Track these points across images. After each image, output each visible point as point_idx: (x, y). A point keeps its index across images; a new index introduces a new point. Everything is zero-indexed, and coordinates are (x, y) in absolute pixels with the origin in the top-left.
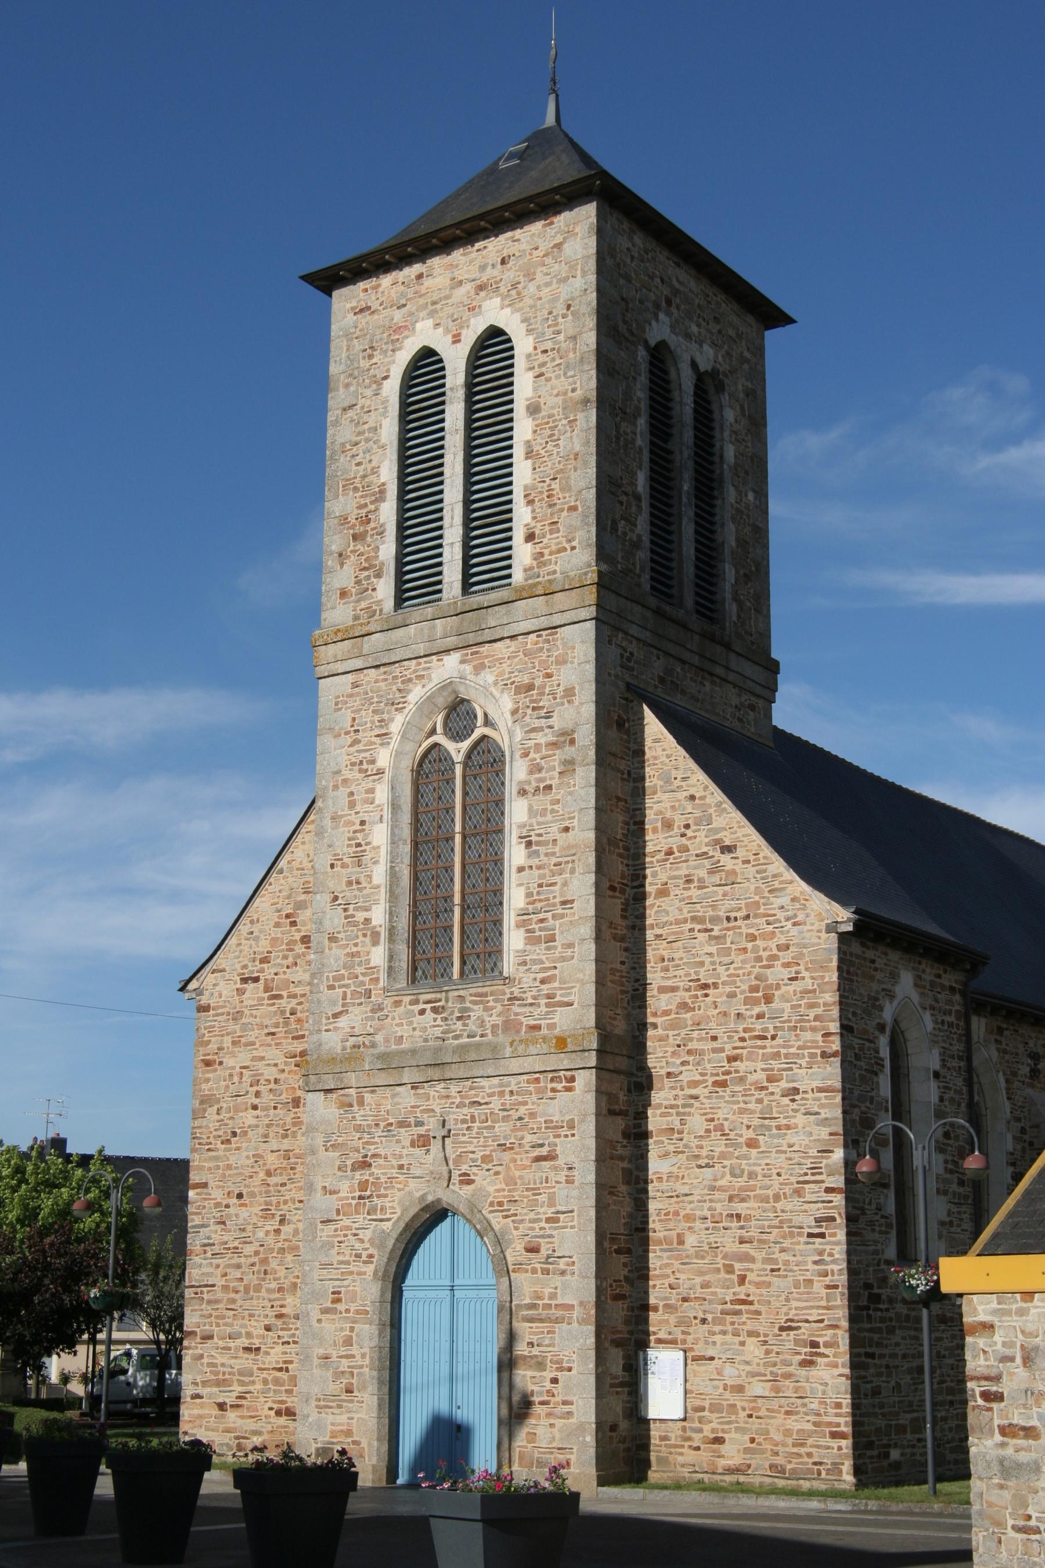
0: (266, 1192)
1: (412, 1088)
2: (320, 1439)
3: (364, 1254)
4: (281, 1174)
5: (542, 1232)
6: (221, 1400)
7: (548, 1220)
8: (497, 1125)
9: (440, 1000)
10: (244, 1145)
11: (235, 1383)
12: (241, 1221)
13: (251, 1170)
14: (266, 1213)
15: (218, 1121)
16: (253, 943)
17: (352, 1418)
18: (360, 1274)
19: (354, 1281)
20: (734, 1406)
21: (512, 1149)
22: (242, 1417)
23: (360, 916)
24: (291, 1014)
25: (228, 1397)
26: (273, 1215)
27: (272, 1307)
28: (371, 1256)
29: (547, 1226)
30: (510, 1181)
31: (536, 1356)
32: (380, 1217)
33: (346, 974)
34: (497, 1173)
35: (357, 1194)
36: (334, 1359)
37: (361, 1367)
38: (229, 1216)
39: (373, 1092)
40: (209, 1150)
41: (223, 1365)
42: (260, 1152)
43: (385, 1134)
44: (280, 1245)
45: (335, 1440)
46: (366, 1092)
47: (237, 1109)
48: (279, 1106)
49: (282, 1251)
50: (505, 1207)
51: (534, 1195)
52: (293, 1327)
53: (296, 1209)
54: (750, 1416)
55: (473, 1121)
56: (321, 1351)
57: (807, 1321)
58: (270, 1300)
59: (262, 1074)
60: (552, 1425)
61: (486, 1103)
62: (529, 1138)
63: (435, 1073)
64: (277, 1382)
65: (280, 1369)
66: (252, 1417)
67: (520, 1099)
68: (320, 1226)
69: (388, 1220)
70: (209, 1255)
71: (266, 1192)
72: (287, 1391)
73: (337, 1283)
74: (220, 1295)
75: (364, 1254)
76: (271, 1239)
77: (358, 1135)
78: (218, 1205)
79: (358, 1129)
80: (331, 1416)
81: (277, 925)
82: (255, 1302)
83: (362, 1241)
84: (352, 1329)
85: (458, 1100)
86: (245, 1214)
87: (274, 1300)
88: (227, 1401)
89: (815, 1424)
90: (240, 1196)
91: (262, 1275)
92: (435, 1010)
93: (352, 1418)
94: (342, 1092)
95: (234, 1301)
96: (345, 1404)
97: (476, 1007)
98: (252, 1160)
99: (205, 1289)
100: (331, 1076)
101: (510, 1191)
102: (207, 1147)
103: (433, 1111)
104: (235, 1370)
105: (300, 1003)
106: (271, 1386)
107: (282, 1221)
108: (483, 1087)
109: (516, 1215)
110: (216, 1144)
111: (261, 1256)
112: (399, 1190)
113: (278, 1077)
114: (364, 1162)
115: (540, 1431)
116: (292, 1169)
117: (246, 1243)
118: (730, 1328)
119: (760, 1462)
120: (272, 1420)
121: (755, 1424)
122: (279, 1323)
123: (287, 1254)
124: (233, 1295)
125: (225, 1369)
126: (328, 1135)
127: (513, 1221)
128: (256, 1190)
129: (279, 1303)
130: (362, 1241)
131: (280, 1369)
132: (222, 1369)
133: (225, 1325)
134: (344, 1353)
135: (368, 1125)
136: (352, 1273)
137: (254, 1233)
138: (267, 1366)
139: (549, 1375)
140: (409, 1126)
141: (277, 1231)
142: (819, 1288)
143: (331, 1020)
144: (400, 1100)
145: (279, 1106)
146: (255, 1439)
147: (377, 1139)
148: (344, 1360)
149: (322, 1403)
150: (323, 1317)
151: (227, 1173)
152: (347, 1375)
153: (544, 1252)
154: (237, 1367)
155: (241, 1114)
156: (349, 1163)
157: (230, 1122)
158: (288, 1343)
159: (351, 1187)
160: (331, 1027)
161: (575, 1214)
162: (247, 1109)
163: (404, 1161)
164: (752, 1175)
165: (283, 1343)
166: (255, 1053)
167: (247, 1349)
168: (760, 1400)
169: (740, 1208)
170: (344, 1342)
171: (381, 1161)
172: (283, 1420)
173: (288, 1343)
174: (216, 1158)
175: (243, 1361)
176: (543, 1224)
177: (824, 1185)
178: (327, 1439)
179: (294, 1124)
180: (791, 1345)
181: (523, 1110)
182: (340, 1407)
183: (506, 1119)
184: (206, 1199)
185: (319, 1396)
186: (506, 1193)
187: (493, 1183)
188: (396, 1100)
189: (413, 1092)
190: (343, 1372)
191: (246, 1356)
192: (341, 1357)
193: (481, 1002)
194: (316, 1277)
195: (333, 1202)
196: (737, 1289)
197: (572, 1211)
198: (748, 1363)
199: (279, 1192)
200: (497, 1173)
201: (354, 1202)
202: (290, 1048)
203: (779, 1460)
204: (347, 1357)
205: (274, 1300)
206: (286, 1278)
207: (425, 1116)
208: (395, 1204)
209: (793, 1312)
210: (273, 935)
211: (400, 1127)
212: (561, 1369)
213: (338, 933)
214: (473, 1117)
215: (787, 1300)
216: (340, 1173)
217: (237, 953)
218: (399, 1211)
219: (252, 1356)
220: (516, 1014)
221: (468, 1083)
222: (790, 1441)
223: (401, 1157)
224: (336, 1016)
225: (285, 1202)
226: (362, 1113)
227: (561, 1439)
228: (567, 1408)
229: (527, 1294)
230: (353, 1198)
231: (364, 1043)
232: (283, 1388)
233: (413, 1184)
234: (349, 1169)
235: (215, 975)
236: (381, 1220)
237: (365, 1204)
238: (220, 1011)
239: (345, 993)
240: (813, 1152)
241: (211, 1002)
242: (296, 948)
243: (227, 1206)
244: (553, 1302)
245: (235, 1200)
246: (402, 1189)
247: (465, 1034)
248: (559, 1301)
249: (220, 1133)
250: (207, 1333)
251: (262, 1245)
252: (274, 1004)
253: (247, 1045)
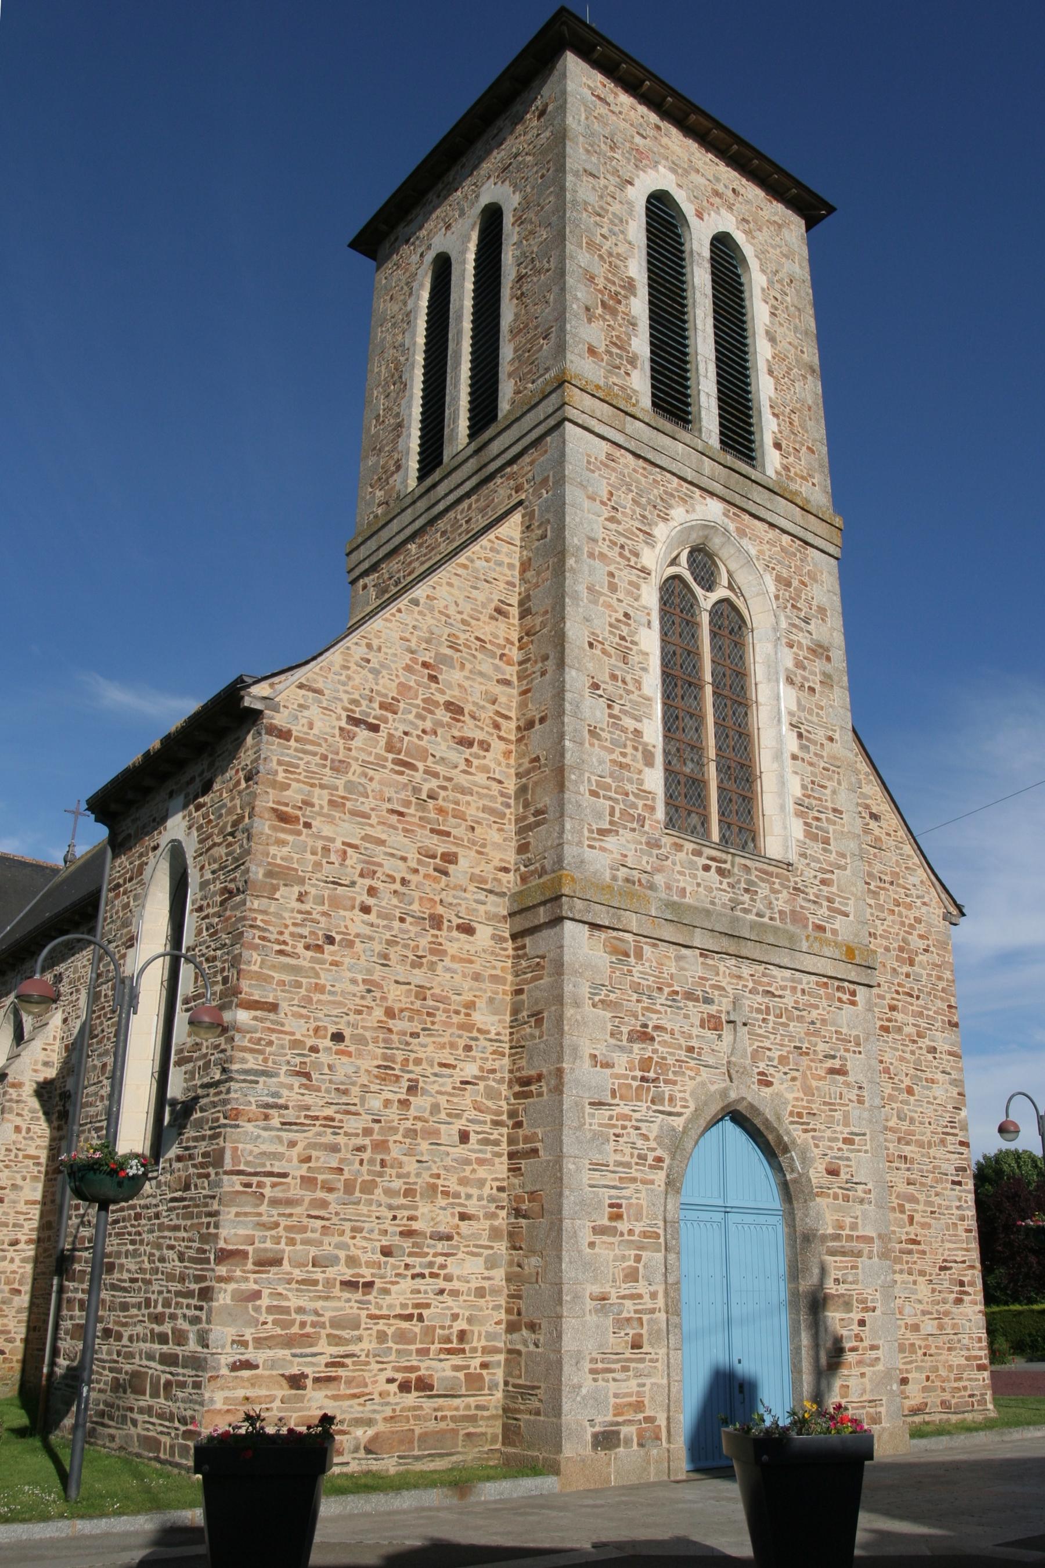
0: (385, 1041)
1: (701, 955)
2: (599, 1419)
3: (651, 1156)
4: (411, 1019)
5: (840, 1154)
6: (295, 1371)
7: (846, 1141)
8: (792, 1024)
9: (725, 862)
10: (347, 960)
11: (323, 1341)
12: (339, 1076)
13: (358, 1001)
14: (386, 1073)
15: (300, 912)
16: (370, 676)
17: (644, 1385)
18: (644, 1182)
19: (637, 1191)
20: (913, 1345)
21: (807, 1054)
22: (335, 1398)
23: (629, 723)
24: (429, 797)
25: (313, 1364)
26: (398, 1077)
27: (395, 1218)
28: (659, 1160)
29: (845, 1147)
30: (808, 1091)
31: (843, 1295)
32: (668, 1109)
33: (614, 785)
34: (794, 1079)
35: (639, 1074)
36: (613, 1300)
37: (652, 1311)
38: (317, 1065)
39: (654, 945)
40: (281, 952)
41: (300, 1310)
42: (376, 977)
43: (669, 1003)
44: (408, 1124)
45: (620, 1419)
46: (646, 943)
47: (336, 903)
48: (409, 919)
49: (411, 1133)
50: (804, 1120)
51: (831, 1110)
52: (431, 1251)
53: (436, 1075)
54: (925, 1354)
55: (768, 1014)
56: (596, 1289)
57: (956, 1262)
58: (390, 1207)
59: (380, 865)
60: (863, 1375)
61: (780, 996)
62: (821, 1047)
63: (725, 944)
64: (402, 1337)
65: (409, 1318)
66: (355, 1396)
67: (812, 1001)
68: (588, 1109)
69: (679, 1114)
70: (275, 1122)
71: (385, 1041)
72: (419, 1352)
73: (613, 1192)
74: (295, 1191)
75: (651, 1156)
76: (393, 1113)
77: (635, 997)
78: (296, 1044)
79: (636, 988)
80: (612, 1383)
81: (408, 668)
82: (364, 1209)
83: (646, 1138)
84: (638, 1259)
85: (750, 985)
86: (357, 1066)
87: (398, 1208)
88: (307, 1370)
89: (968, 1359)
90: (338, 1037)
91: (378, 1168)
92: (721, 872)
93: (644, 1385)
94: (615, 934)
95: (324, 1204)
96: (633, 1365)
97: (763, 885)
98: (362, 987)
99: (268, 1180)
100: (604, 908)
101: (808, 1102)
102: (277, 947)
103: (724, 989)
104: (325, 1319)
105: (445, 788)
106: (390, 1344)
107: (412, 1089)
108: (774, 977)
109: (815, 1130)
110: (294, 947)
111: (375, 1137)
112: (692, 1078)
113: (408, 877)
114: (645, 1033)
115: (852, 1382)
116: (429, 1014)
117: (348, 1113)
118: (905, 1267)
119: (934, 1399)
120: (392, 1399)
121: (929, 1362)
122: (407, 1244)
123: (419, 1140)
124: (320, 1194)
125: (305, 1318)
126: (596, 987)
127: (813, 1137)
128: (368, 1034)
129: (406, 1213)
130: (646, 1138)
131: (409, 1318)
132: (299, 1318)
133: (304, 1242)
134: (627, 1292)
135: (649, 987)
136: (634, 1180)
137: (363, 1100)
138: (385, 1312)
139: (856, 1316)
140: (697, 1000)
141: (404, 1104)
142: (960, 1231)
143: (595, 835)
144: (687, 966)
145: (409, 919)
146: (359, 1432)
147: (658, 1007)
148: (628, 1303)
149: (600, 1365)
150: (597, 1239)
151: (316, 997)
152: (635, 1324)
153: (844, 1176)
154: (328, 1314)
155: (342, 913)
156: (625, 1030)
157: (323, 919)
158: (422, 1276)
159: (631, 1062)
160: (597, 844)
161: (868, 1137)
162: (353, 907)
163: (693, 1043)
164: (912, 1121)
165: (413, 1277)
166: (370, 831)
167: (350, 1285)
168: (930, 1338)
169: (908, 1150)
170: (626, 1276)
171: (667, 1037)
172: (411, 1398)
173: (422, 1276)
174: (296, 970)
175: (342, 1304)
176: (840, 1145)
177: (959, 1138)
178: (609, 1418)
179: (433, 952)
180: (946, 1284)
181: (815, 1013)
182: (626, 1369)
183: (800, 1019)
184: (273, 1031)
185: (594, 1355)
186: (805, 1103)
187: (790, 1089)
188: (682, 964)
189: (701, 959)
190: (628, 1320)
191: (346, 1295)
192: (623, 1297)
193: (768, 881)
194: (586, 1181)
195: (604, 1079)
196: (908, 1229)
197: (864, 1135)
198: (920, 1302)
199: (408, 1044)
200: (794, 1079)
201: (635, 1084)
202: (427, 842)
203: (947, 1396)
204: (632, 1297)
205: (398, 1208)
206: (418, 1175)
207: (716, 993)
208: (687, 1095)
209: (947, 1253)
210: (402, 680)
211: (687, 999)
212: (866, 1309)
213: (602, 730)
214: (767, 1008)
215: (942, 1241)
216: (613, 1041)
217: (343, 678)
218: (692, 1106)
219: (359, 1295)
220: (802, 907)
221: (761, 968)
222: (952, 1376)
223: (690, 1037)
224: (602, 832)
225: (418, 1062)
226: (640, 968)
227: (872, 1390)
228: (874, 1354)
229: (830, 1223)
230: (634, 1078)
231: (639, 881)
232: (413, 1347)
233: (705, 1074)
234: (625, 1037)
235: (303, 692)
236: (670, 1114)
237: (648, 1088)
238: (309, 747)
239: (612, 809)
240: (950, 1108)
241: (293, 728)
242: (437, 711)
243: (314, 1049)
244: (855, 1233)
245: (328, 1043)
246: (694, 1078)
247: (755, 911)
248: (860, 1233)
249: (305, 931)
250: (270, 1255)
251: (379, 1121)
252: (402, 773)
253: (354, 813)
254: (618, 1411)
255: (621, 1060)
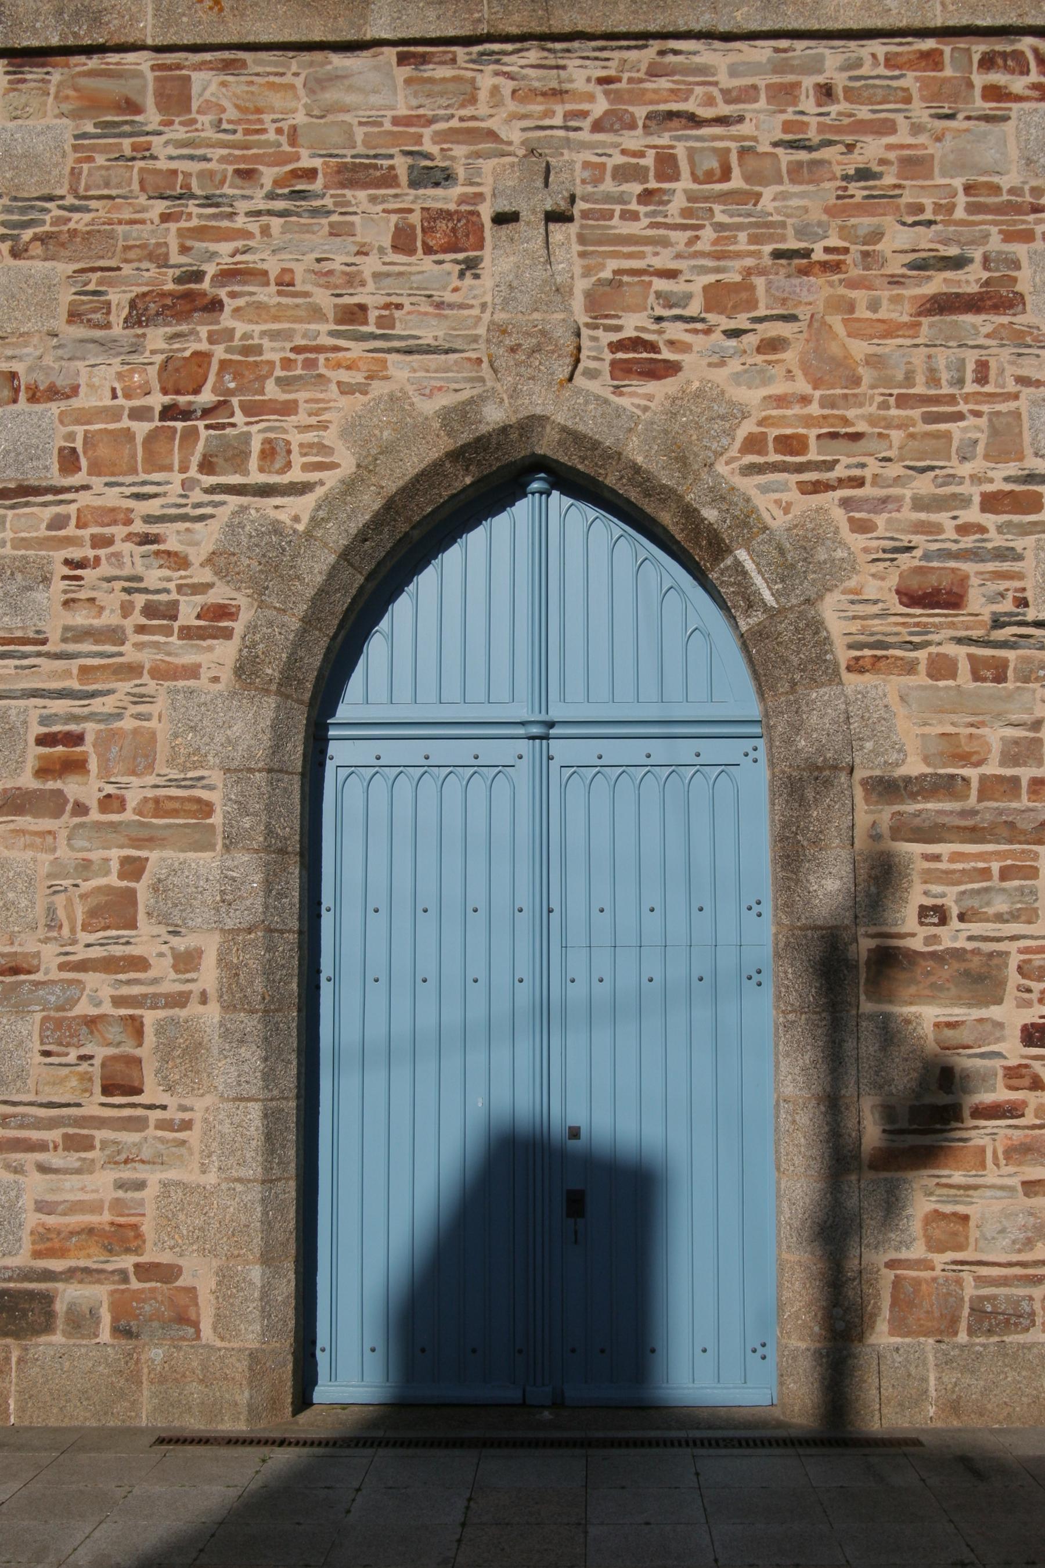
5: (968, 542)
7: (991, 503)
8: (768, 192)
17: (140, 1185)
19: (140, 699)
21: (836, 267)
28: (223, 612)
29: (990, 520)
30: (832, 372)
31: (958, 954)
32: (256, 477)
34: (772, 346)
35: (157, 400)
37: (180, 1000)
39: (227, 66)
43: (280, 205)
46: (199, 67)
61: (722, 121)
67: (863, 113)
73: (60, 706)
77: (161, 206)
79: (171, 191)
84: (133, 868)
85: (600, 106)
93: (140, 1185)
94: (94, 62)
96: (100, 1135)
101: (828, 402)
103: (492, 135)
108: (703, 70)
112: (346, 390)
136: (133, 670)
140: (389, 179)
144: (350, 99)
147: (240, 222)
148: (91, 979)
152: (114, 1032)
153: (979, 604)
156: (119, 298)
171: (267, 294)
181: (872, 149)
182: (76, 1144)
186: (814, 409)
188: (331, 96)
189: (407, 71)
190: (91, 1022)
192: (83, 966)
200: (772, 346)
201: (141, 429)
204: (109, 965)
207: (460, 151)
218: (347, 462)
221: (649, 53)
223: (353, 279)
226: (179, 132)
229: (912, 746)
230: (139, 414)
233: (401, 370)
234: (117, 318)
236: (266, 491)
237: (193, 432)
254: (49, 1243)
255: (98, 381)
